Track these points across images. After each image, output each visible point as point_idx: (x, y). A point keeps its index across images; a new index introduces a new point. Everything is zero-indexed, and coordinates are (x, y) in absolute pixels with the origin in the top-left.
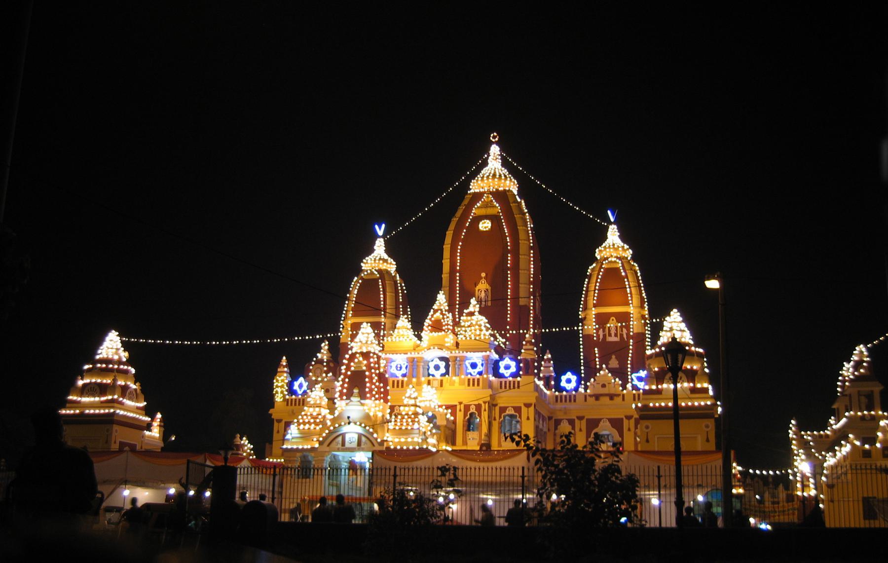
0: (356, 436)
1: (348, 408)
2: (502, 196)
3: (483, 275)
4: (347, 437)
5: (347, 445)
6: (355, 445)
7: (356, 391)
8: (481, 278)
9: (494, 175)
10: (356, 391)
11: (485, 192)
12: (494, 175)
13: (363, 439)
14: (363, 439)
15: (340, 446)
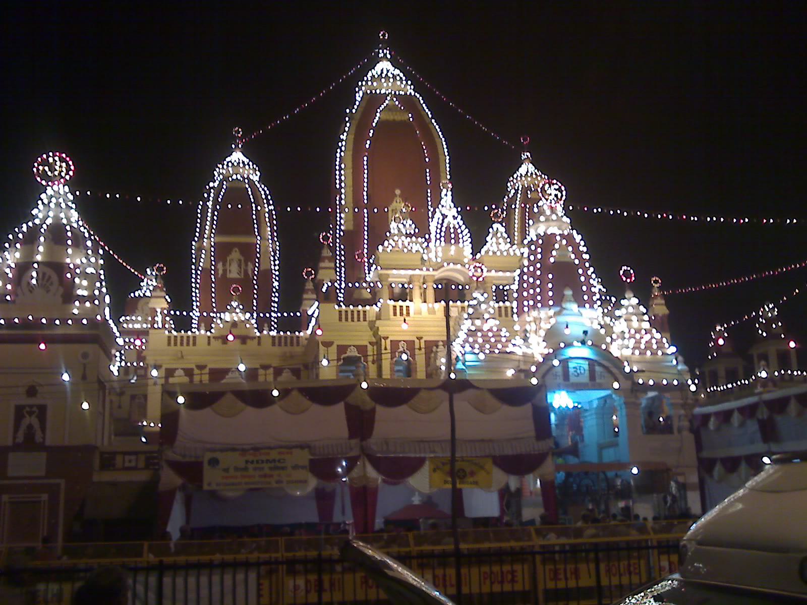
0: (585, 365)
1: (562, 319)
2: (406, 100)
3: (398, 192)
4: (572, 365)
5: (573, 379)
6: (585, 379)
7: (568, 292)
8: (396, 195)
9: (386, 76)
10: (568, 292)
11: (386, 95)
12: (386, 76)
13: (598, 368)
14: (598, 368)
15: (560, 380)
